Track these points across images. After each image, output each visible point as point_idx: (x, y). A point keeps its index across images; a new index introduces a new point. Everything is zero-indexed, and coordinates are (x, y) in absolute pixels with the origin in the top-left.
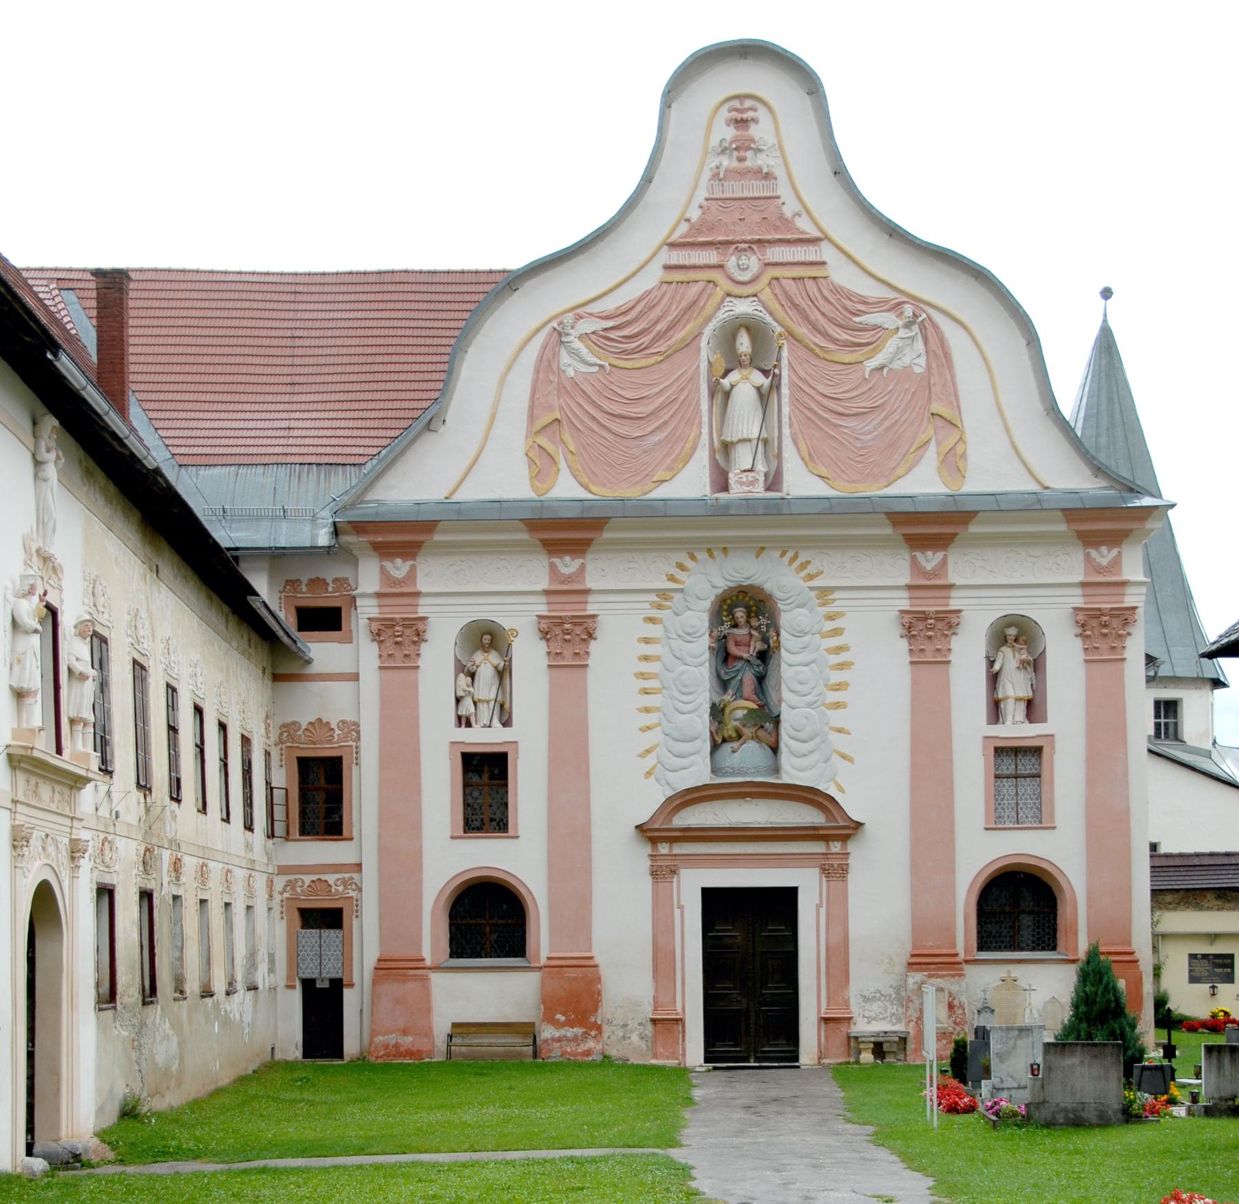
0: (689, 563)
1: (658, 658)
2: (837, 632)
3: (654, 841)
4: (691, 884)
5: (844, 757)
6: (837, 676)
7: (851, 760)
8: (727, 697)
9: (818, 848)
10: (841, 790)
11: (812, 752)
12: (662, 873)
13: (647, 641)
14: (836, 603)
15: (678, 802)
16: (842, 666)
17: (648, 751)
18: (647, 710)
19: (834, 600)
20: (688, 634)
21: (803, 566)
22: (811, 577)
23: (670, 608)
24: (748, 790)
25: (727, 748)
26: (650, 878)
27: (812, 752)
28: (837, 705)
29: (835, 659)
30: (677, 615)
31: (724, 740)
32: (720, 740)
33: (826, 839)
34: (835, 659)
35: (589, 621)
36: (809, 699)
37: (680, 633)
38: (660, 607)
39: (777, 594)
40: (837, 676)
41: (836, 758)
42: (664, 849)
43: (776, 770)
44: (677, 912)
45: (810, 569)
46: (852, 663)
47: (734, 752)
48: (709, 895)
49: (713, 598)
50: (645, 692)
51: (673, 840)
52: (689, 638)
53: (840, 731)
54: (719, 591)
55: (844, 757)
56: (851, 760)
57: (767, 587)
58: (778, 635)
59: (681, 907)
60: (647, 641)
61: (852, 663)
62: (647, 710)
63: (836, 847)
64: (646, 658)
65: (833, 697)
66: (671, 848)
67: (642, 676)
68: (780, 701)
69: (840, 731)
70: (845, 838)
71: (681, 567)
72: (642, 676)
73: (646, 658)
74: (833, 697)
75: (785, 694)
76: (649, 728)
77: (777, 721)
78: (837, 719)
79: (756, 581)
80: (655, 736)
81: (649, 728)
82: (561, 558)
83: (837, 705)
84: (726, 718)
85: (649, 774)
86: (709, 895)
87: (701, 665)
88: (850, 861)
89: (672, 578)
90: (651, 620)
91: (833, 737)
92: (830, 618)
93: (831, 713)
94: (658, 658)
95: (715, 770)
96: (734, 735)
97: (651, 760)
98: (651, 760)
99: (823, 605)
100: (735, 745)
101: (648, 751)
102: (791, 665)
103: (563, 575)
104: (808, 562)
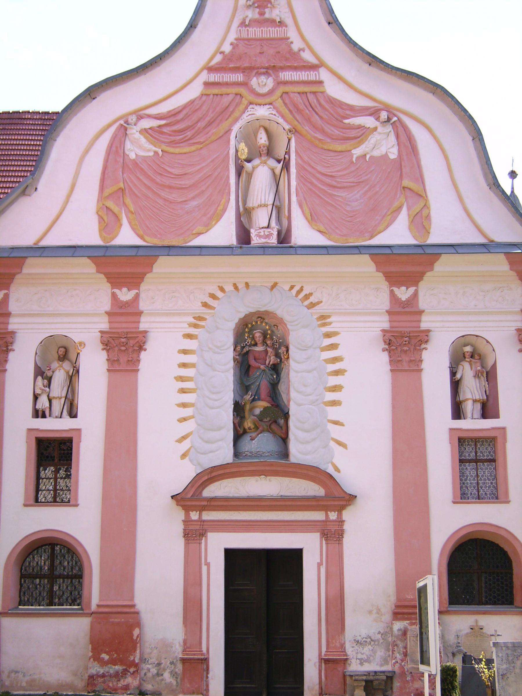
0: (219, 294)
1: (193, 365)
2: (333, 347)
3: (187, 509)
4: (217, 545)
5: (339, 443)
6: (333, 381)
7: (344, 446)
8: (248, 397)
9: (318, 516)
10: (337, 470)
11: (314, 439)
12: (194, 534)
13: (185, 352)
14: (332, 325)
15: (206, 478)
16: (337, 373)
17: (184, 438)
18: (184, 405)
19: (330, 323)
20: (218, 347)
21: (307, 297)
22: (312, 305)
23: (203, 327)
24: (263, 468)
26: (183, 540)
27: (314, 439)
28: (335, 403)
29: (331, 367)
30: (209, 332)
31: (245, 432)
32: (241, 432)
33: (326, 509)
34: (331, 367)
35: (140, 336)
36: (311, 398)
37: (210, 346)
38: (196, 326)
39: (287, 318)
40: (333, 381)
41: (332, 444)
42: (194, 516)
43: (285, 454)
44: (204, 569)
45: (312, 299)
46: (345, 371)
47: (252, 439)
48: (231, 555)
49: (237, 321)
50: (183, 391)
51: (202, 509)
52: (217, 350)
53: (336, 423)
54: (242, 316)
55: (339, 443)
56: (344, 446)
57: (280, 313)
58: (287, 351)
59: (208, 565)
60: (185, 352)
61: (345, 371)
62: (184, 405)
63: (333, 516)
64: (184, 365)
65: (330, 396)
66: (200, 515)
67: (181, 379)
68: (289, 401)
69: (336, 423)
70: (340, 509)
71: (213, 296)
72: (181, 379)
73: (184, 365)
74: (330, 396)
76: (185, 419)
77: (286, 416)
78: (333, 413)
79: (270, 308)
80: (190, 426)
81: (185, 419)
82: (120, 289)
83: (335, 403)
84: (247, 414)
85: (184, 456)
86: (231, 555)
87: (227, 371)
88: (345, 527)
89: (205, 305)
90: (189, 336)
91: (331, 427)
92: (328, 335)
93: (329, 409)
94: (193, 365)
95: (236, 454)
96: (252, 426)
97: (186, 445)
98: (186, 445)
99: (324, 325)
100: (254, 435)
101: (184, 438)
102: (297, 372)
103: (122, 302)
104: (311, 294)
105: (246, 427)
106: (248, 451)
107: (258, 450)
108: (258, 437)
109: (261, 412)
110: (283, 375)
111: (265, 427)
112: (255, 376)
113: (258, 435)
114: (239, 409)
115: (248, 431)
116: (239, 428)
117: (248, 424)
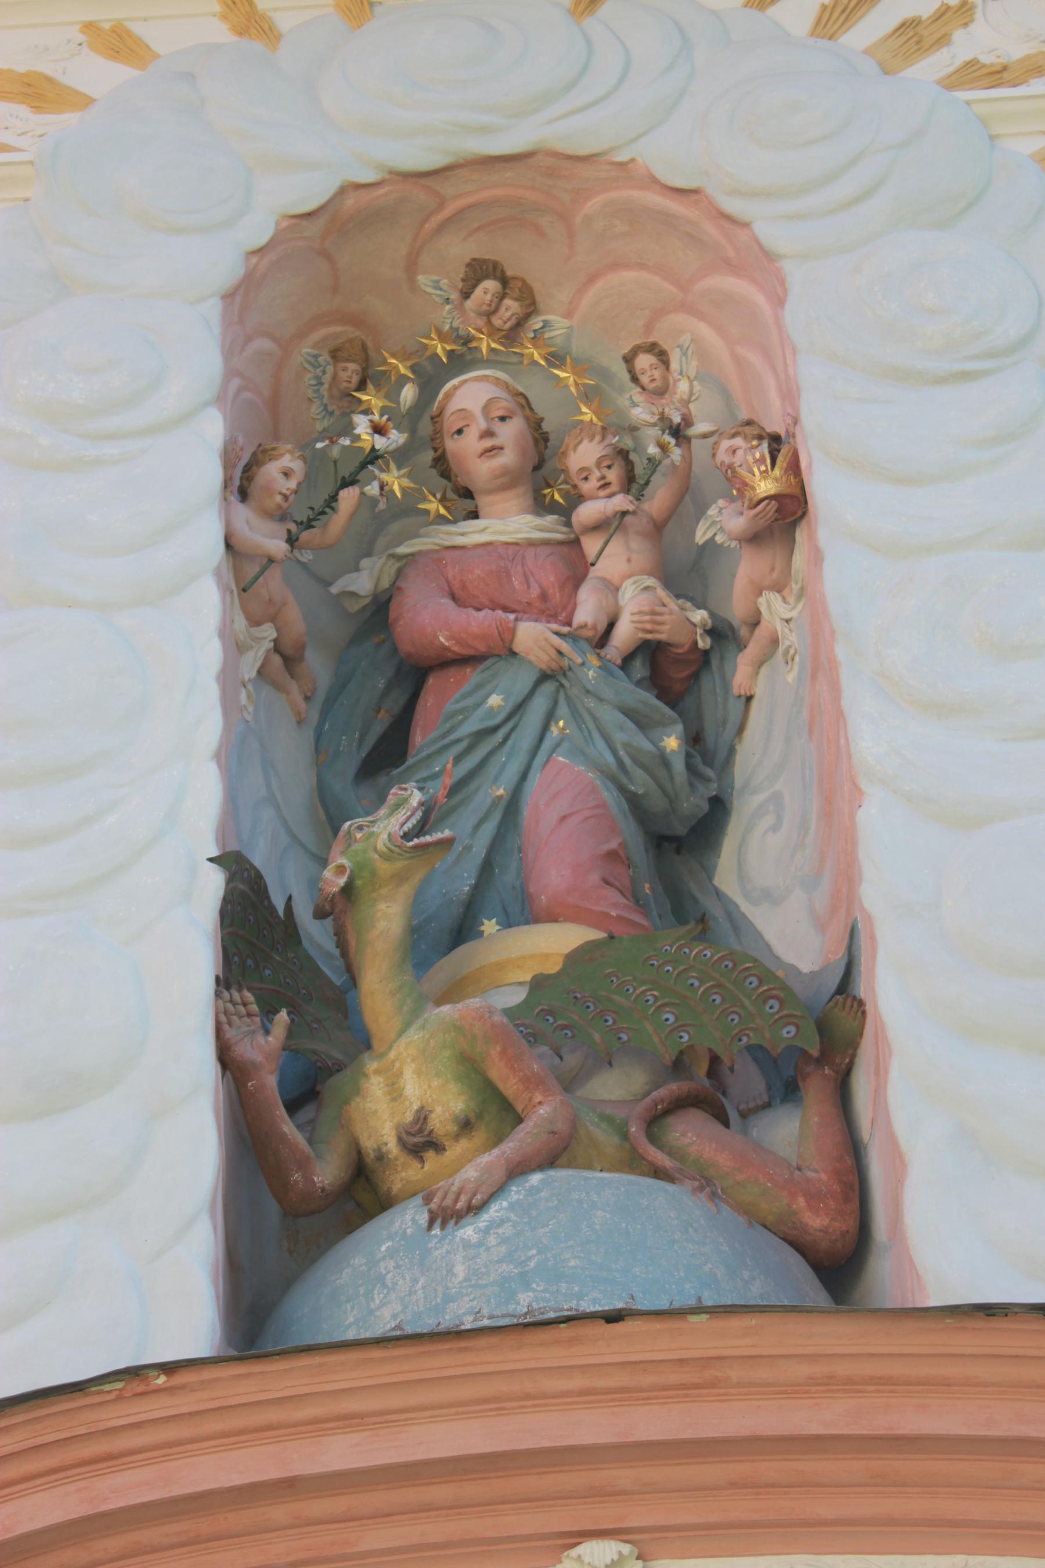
96: (448, 1102)
108: (516, 1192)
114: (264, 948)
117: (395, 1093)
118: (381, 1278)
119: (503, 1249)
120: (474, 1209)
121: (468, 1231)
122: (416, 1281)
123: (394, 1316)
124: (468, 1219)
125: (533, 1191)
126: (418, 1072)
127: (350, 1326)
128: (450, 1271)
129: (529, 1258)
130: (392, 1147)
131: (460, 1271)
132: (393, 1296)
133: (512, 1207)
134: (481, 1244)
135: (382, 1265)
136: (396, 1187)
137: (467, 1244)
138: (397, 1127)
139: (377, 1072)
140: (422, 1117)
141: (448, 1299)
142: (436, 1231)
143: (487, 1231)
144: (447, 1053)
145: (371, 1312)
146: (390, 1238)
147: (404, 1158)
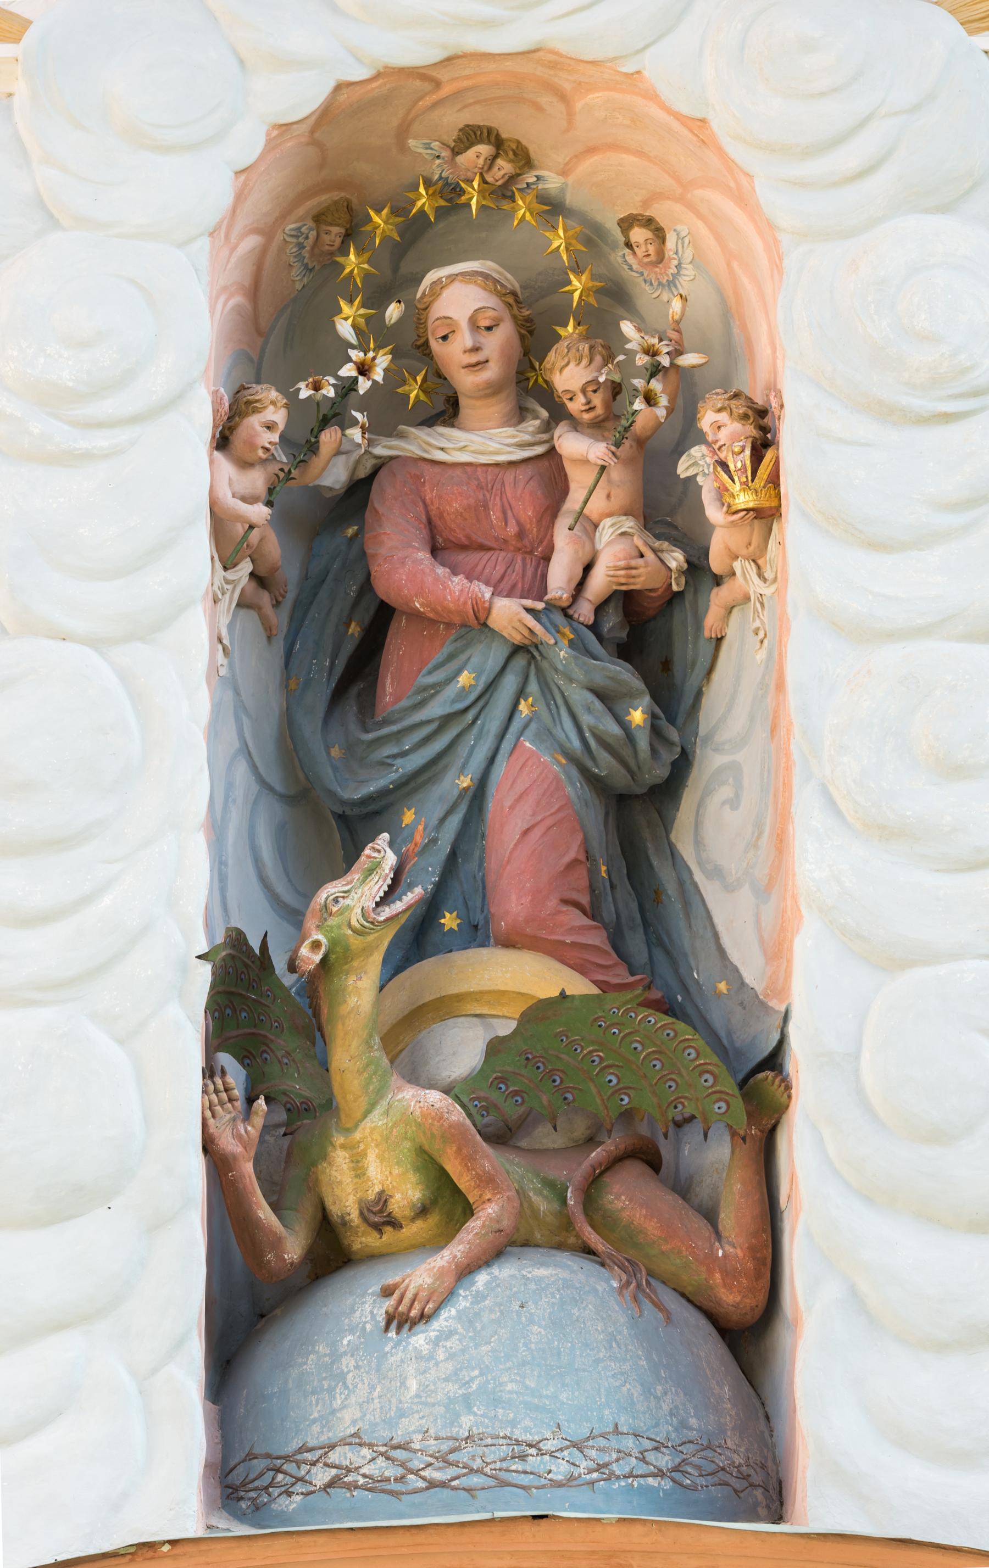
8: (359, 896)
25: (356, 1304)
31: (331, 1254)
32: (294, 1247)
47: (400, 1321)
75: (821, 858)
96: (407, 1193)
100: (421, 1274)
105: (346, 1199)
106: (356, 1440)
107: (466, 1423)
108: (463, 1300)
109: (495, 1047)
110: (729, 703)
111: (543, 1204)
112: (436, 709)
113: (466, 1271)
115: (364, 1240)
116: (264, 1213)
117: (359, 1171)
118: (342, 1377)
119: (450, 1366)
120: (424, 1317)
121: (420, 1339)
122: (373, 1388)
123: (354, 1422)
124: (420, 1327)
125: (479, 1297)
126: (381, 1158)
127: (315, 1421)
128: (403, 1384)
129: (472, 1379)
130: (354, 1216)
131: (413, 1385)
132: (353, 1400)
133: (459, 1317)
134: (431, 1357)
135: (344, 1361)
136: (356, 1247)
137: (419, 1357)
138: (360, 1202)
139: (343, 1147)
140: (383, 1199)
141: (402, 1414)
142: (392, 1334)
143: (436, 1342)
144: (407, 1144)
145: (333, 1412)
146: (352, 1331)
147: (363, 1227)
